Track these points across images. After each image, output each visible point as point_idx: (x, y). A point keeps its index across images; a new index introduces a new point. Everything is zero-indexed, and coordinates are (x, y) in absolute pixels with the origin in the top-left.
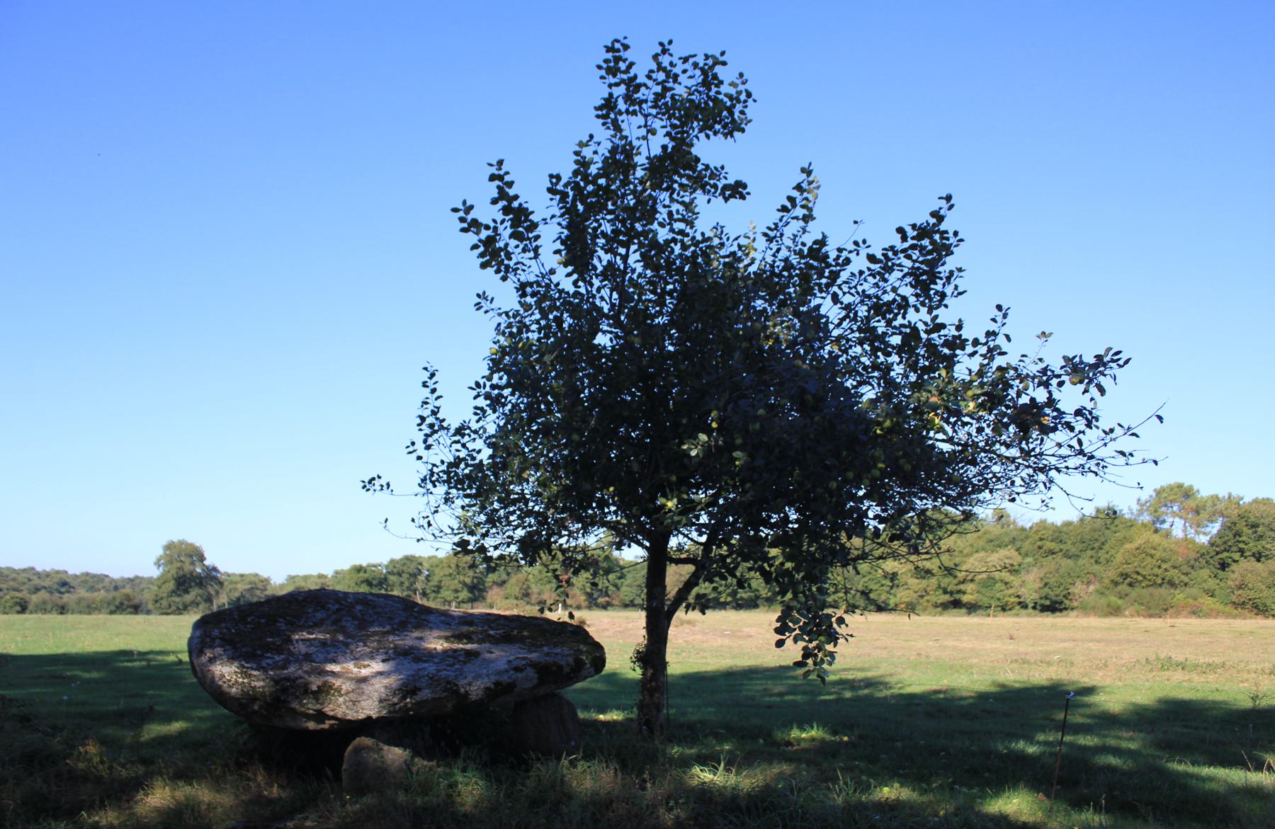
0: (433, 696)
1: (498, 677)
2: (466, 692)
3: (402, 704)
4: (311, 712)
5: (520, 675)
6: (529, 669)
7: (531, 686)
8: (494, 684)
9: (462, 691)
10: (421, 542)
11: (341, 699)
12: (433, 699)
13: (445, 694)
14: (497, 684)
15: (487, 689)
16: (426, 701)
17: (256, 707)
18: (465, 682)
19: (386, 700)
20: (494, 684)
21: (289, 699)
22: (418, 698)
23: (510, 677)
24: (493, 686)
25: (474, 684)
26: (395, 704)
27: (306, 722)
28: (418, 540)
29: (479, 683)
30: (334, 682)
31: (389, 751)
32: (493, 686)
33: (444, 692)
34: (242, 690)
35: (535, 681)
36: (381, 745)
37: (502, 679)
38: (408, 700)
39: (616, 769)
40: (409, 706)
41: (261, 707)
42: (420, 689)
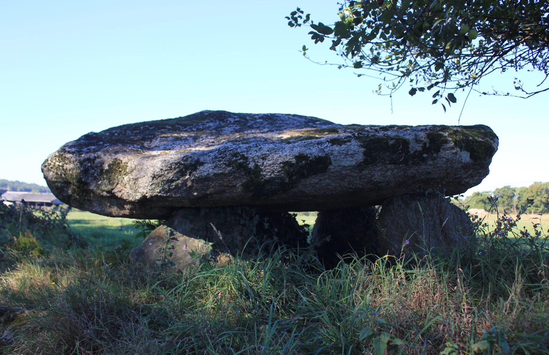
0: (215, 171)
1: (304, 149)
2: (257, 166)
3: (179, 181)
4: (105, 194)
5: (336, 148)
6: (353, 142)
7: (354, 163)
8: (296, 157)
9: (252, 165)
10: (343, 68)
11: (126, 178)
12: (215, 175)
13: (229, 169)
14: (300, 157)
15: (286, 163)
16: (206, 179)
17: (70, 192)
18: (259, 154)
19: (160, 176)
20: (296, 157)
21: (89, 181)
22: (197, 174)
23: (322, 150)
24: (294, 161)
25: (270, 157)
26: (172, 181)
27: (110, 207)
28: (340, 67)
29: (276, 157)
30: (122, 159)
31: (185, 242)
32: (294, 161)
33: (229, 165)
34: (57, 174)
35: (360, 157)
36: (178, 235)
37: (308, 152)
38: (187, 177)
39: (20, 244)
40: (189, 184)
41: (74, 191)
42: (202, 164)
